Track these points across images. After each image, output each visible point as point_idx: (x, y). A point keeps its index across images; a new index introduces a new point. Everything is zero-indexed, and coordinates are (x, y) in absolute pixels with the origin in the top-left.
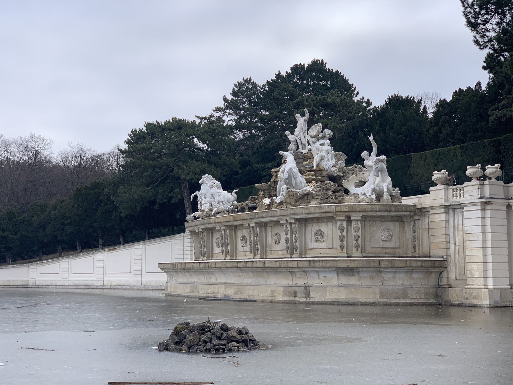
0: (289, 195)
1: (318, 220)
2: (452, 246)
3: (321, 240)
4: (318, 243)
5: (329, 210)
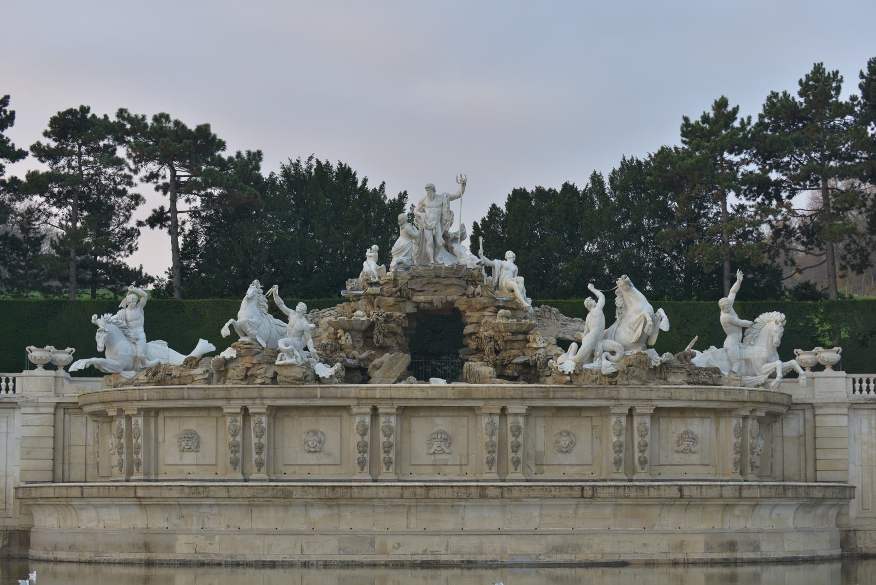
0: (640, 362)
1: (682, 412)
2: (852, 468)
3: (693, 449)
4: (681, 455)
5: (740, 398)
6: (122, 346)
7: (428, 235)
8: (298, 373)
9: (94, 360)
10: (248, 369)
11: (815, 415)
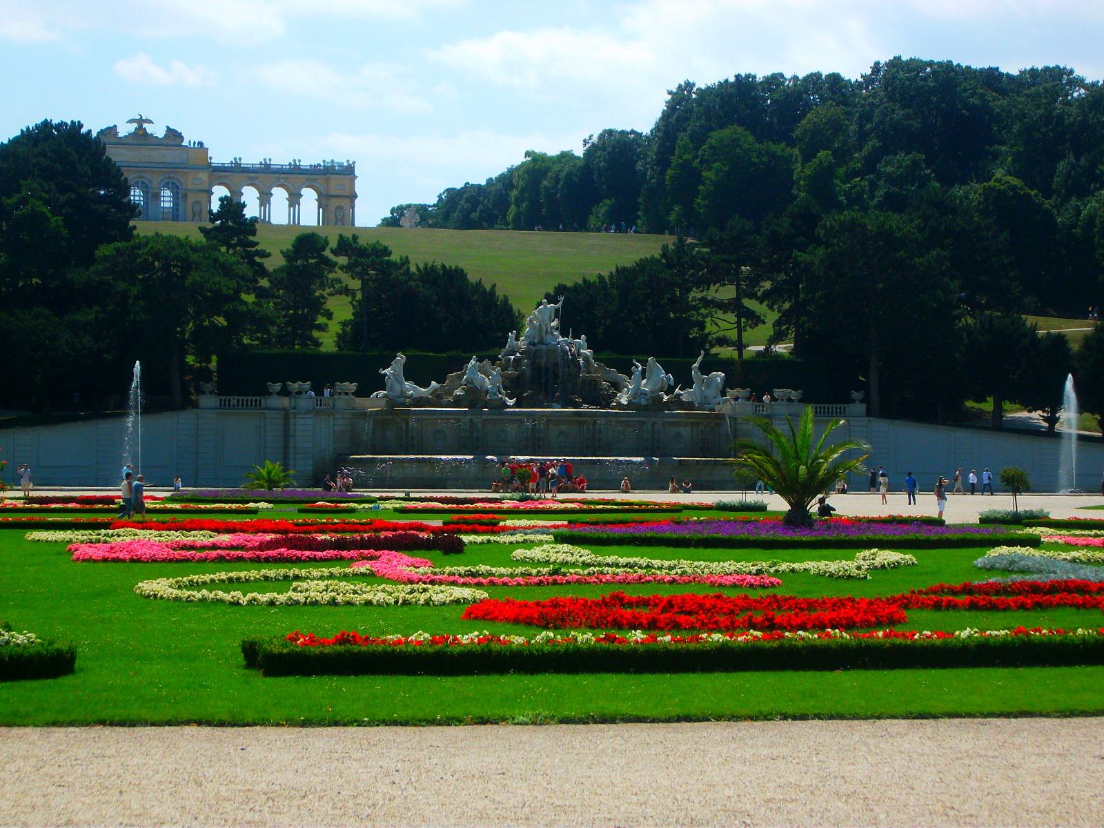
6: (397, 387)
7: (543, 326)
8: (499, 403)
9: (382, 393)
10: (472, 400)
11: (736, 424)
